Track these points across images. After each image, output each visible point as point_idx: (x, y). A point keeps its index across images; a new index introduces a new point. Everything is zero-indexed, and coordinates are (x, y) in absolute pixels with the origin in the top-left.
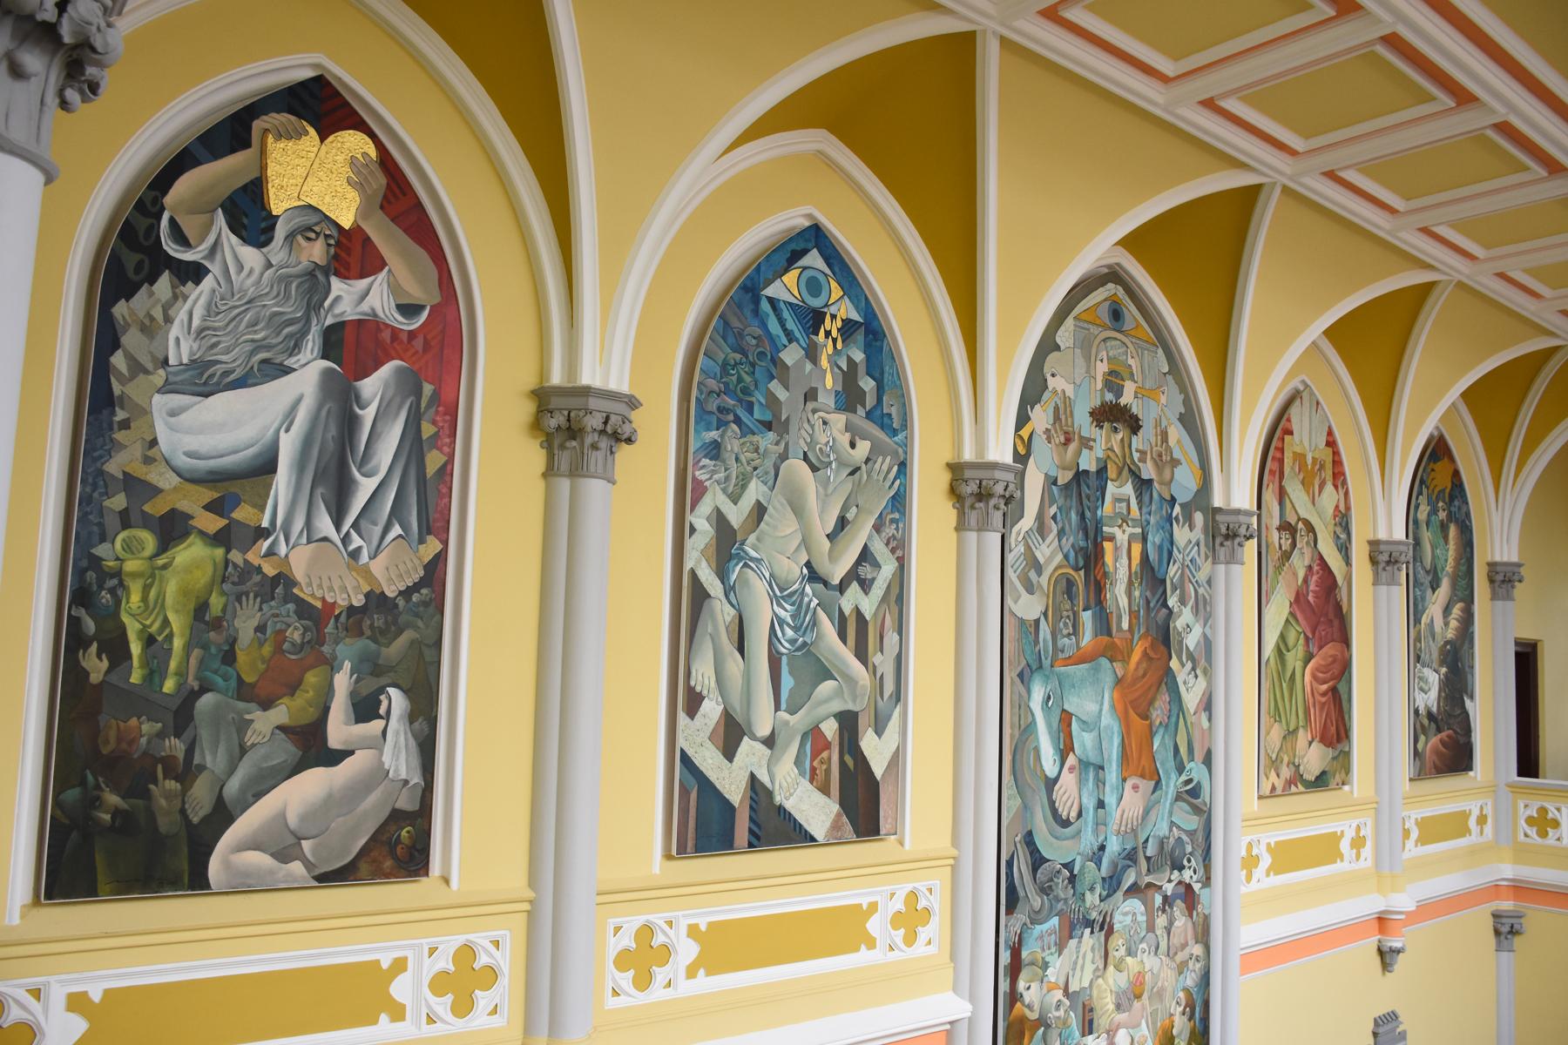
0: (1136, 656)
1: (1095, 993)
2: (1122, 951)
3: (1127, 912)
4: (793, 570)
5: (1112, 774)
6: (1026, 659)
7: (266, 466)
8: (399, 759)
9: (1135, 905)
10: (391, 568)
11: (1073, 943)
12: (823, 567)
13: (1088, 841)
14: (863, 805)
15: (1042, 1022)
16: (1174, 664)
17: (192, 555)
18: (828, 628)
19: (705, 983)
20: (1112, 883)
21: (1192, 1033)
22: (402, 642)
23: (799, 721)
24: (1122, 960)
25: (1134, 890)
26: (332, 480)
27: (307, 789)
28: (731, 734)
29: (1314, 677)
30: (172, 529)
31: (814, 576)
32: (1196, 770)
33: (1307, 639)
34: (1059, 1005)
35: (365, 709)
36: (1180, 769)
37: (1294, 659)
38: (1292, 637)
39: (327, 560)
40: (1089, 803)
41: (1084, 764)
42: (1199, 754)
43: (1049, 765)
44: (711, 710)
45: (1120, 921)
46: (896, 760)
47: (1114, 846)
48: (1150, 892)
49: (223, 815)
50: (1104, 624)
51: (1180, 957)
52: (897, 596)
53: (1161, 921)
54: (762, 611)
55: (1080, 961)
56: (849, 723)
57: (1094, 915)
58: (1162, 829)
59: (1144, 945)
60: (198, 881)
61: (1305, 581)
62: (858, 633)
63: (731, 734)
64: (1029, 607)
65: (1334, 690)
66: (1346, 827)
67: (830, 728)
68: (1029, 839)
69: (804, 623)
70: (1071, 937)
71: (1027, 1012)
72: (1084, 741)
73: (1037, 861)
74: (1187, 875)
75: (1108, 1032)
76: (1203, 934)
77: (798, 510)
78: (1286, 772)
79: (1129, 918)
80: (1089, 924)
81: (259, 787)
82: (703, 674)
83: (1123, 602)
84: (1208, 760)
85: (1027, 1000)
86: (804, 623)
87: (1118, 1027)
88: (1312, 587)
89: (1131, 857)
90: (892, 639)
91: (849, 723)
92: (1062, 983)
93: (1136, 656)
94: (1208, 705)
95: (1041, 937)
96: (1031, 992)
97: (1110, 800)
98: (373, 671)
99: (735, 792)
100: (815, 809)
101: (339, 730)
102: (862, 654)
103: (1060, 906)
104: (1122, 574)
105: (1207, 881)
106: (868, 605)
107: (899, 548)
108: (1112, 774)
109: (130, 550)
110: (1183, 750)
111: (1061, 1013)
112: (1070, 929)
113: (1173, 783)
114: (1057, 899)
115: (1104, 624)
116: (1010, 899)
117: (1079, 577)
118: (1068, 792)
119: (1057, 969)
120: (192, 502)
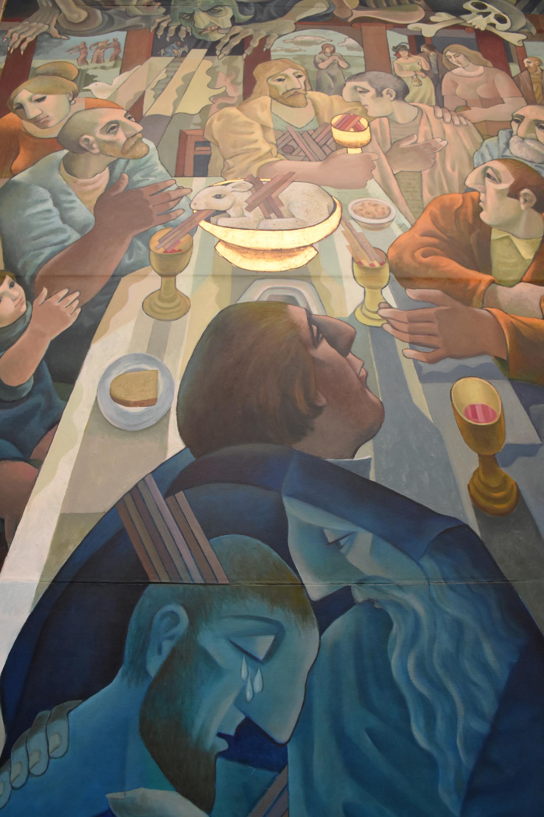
1: (216, 123)
2: (299, 83)
11: (159, 63)
24: (295, 93)
34: (112, 127)
45: (278, 48)
48: (369, 30)
51: (477, 113)
55: (177, 81)
57: (216, 36)
59: (365, 84)
70: (155, 52)
71: (31, 128)
75: (255, 182)
79: (319, 48)
80: (212, 50)
85: (33, 110)
87: (288, 178)
92: (126, 99)
95: (83, 48)
103: (130, 22)
111: (121, 137)
114: (127, 15)
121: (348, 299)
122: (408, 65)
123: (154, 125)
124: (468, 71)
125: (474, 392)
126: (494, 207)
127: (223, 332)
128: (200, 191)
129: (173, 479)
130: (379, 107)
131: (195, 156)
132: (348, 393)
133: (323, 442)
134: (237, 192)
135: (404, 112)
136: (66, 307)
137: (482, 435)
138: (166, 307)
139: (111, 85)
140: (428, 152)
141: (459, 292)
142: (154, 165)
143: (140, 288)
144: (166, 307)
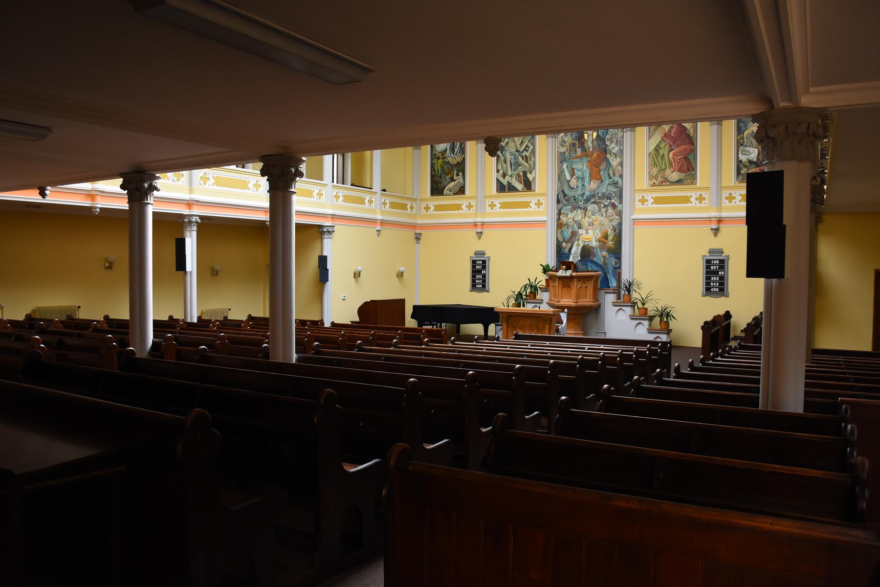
0: (595, 155)
3: (591, 207)
4: (514, 150)
5: (587, 180)
6: (562, 159)
7: (446, 150)
8: (461, 181)
9: (595, 206)
10: (459, 159)
12: (519, 149)
13: (580, 192)
14: (528, 185)
15: (567, 224)
16: (608, 156)
17: (440, 160)
18: (520, 158)
19: (501, 210)
20: (587, 201)
21: (615, 235)
22: (461, 167)
23: (516, 173)
25: (594, 203)
26: (453, 150)
27: (452, 184)
28: (504, 175)
29: (674, 154)
30: (439, 158)
31: (517, 151)
32: (616, 179)
33: (670, 146)
35: (458, 175)
36: (610, 178)
37: (664, 151)
38: (662, 145)
39: (453, 159)
40: (580, 185)
41: (578, 178)
42: (617, 174)
43: (568, 177)
44: (501, 172)
46: (534, 178)
47: (587, 193)
49: (445, 187)
50: (584, 150)
52: (533, 152)
53: (603, 210)
54: (509, 157)
56: (525, 173)
58: (604, 191)
60: (442, 194)
61: (670, 130)
62: (526, 159)
63: (504, 175)
64: (563, 150)
65: (686, 158)
66: (694, 195)
67: (521, 174)
68: (563, 191)
69: (516, 158)
72: (578, 173)
73: (565, 195)
74: (613, 201)
76: (620, 214)
77: (514, 141)
78: (660, 179)
81: (448, 184)
82: (500, 167)
83: (590, 145)
84: (621, 176)
86: (516, 158)
88: (673, 131)
89: (594, 196)
90: (533, 159)
91: (525, 173)
93: (595, 155)
94: (621, 164)
96: (564, 219)
97: (586, 184)
98: (458, 171)
99: (505, 183)
100: (519, 186)
101: (455, 178)
102: (527, 162)
104: (590, 139)
105: (621, 202)
106: (527, 154)
107: (534, 144)
108: (587, 180)
109: (435, 161)
110: (611, 174)
112: (574, 208)
113: (607, 181)
115: (584, 150)
116: (558, 202)
117: (577, 143)
118: (573, 183)
119: (570, 215)
120: (440, 155)
121: (594, 244)
122: (603, 210)
123: (576, 222)
124: (610, 210)
125: (604, 253)
126: (610, 232)
127: (583, 247)
128: (581, 231)
129: (580, 261)
130: (599, 218)
131: (580, 227)
132: (594, 253)
133: (591, 258)
134: (584, 231)
135: (602, 218)
136: (569, 245)
137: (604, 257)
138: (578, 245)
139: (570, 215)
140: (603, 225)
141: (604, 243)
142: (576, 229)
143: (576, 243)
144: (578, 245)
